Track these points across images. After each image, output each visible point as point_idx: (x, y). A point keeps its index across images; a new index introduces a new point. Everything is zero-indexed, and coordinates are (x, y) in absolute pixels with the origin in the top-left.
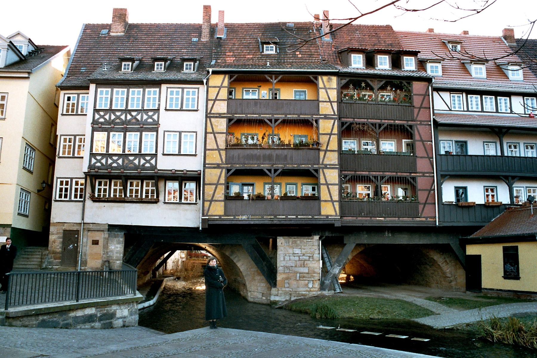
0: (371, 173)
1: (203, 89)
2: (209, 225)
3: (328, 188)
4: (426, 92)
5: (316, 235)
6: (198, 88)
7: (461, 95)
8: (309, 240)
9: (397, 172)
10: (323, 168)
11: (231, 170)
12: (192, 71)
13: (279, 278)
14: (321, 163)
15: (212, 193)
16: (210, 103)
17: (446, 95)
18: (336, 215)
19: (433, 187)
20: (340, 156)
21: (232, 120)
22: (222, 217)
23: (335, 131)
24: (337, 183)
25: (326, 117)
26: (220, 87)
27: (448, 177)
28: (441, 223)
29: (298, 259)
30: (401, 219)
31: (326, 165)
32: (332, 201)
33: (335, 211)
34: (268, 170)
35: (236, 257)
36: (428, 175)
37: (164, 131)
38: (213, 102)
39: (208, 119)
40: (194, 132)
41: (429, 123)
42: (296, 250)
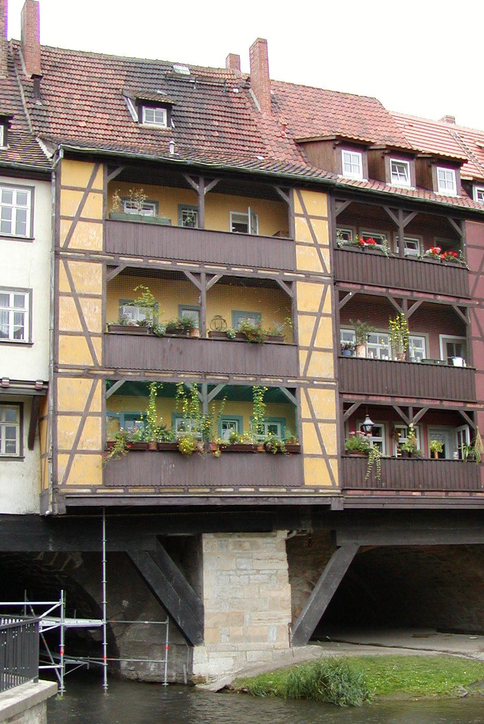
0: (397, 400)
2: (69, 508)
5: (282, 529)
10: (306, 387)
14: (301, 374)
15: (73, 433)
20: (339, 362)
22: (99, 491)
23: (328, 308)
25: (309, 277)
26: (88, 190)
29: (246, 581)
30: (450, 494)
31: (312, 380)
32: (326, 457)
33: (332, 477)
40: (25, 290)
42: (243, 561)
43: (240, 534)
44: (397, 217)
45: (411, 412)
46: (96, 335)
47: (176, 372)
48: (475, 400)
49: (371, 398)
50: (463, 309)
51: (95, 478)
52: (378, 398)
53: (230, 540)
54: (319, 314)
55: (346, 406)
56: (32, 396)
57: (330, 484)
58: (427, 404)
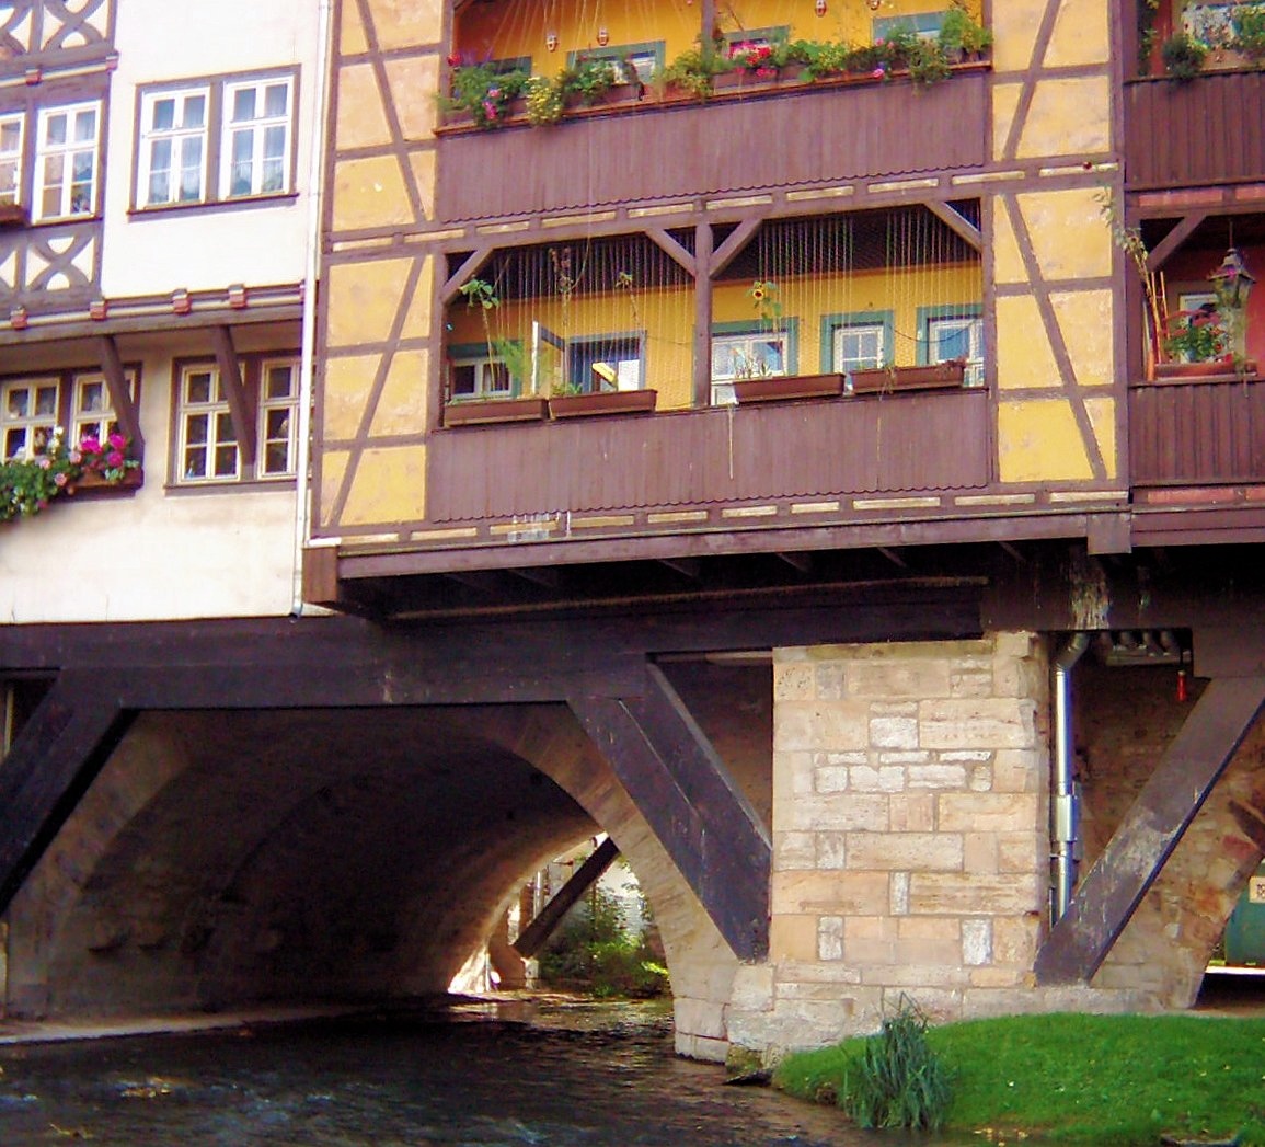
3: (1047, 312)
5: (1013, 627)
8: (970, 664)
10: (1012, 189)
11: (468, 255)
13: (784, 900)
14: (998, 156)
15: (362, 396)
18: (1100, 482)
20: (1127, 98)
29: (899, 781)
33: (1094, 453)
34: (672, 232)
35: (606, 796)
37: (142, 88)
40: (284, 70)
42: (889, 723)
46: (420, 145)
47: (622, 205)
49: (1243, 193)
51: (411, 507)
53: (853, 664)
55: (1153, 230)
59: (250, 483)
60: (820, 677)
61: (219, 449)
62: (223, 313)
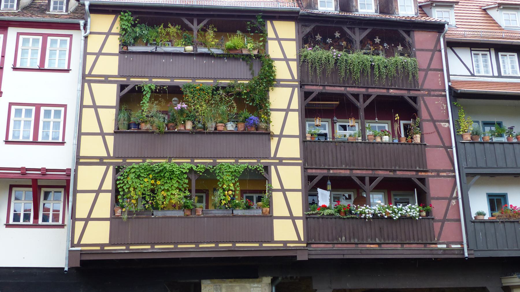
0: (354, 172)
1: (78, 36)
2: (82, 262)
4: (436, 46)
6: (71, 36)
7: (488, 53)
8: (256, 285)
9: (395, 171)
10: (275, 165)
12: (64, 13)
14: (272, 156)
16: (90, 59)
17: (465, 54)
18: (300, 241)
19: (455, 195)
21: (127, 86)
23: (295, 105)
24: (300, 188)
26: (108, 34)
27: (477, 177)
28: (472, 252)
30: (405, 246)
31: (281, 159)
32: (293, 218)
36: (445, 174)
37: (11, 104)
38: (94, 57)
39: (86, 85)
41: (443, 93)
43: (232, 280)
44: (354, 33)
45: (367, 180)
48: (427, 168)
49: (331, 171)
50: (414, 99)
51: (105, 239)
52: (338, 171)
53: (224, 285)
54: (288, 110)
56: (66, 180)
57: (296, 239)
58: (382, 174)
59: (36, 225)
60: (215, 288)
61: (24, 214)
62: (37, 175)
